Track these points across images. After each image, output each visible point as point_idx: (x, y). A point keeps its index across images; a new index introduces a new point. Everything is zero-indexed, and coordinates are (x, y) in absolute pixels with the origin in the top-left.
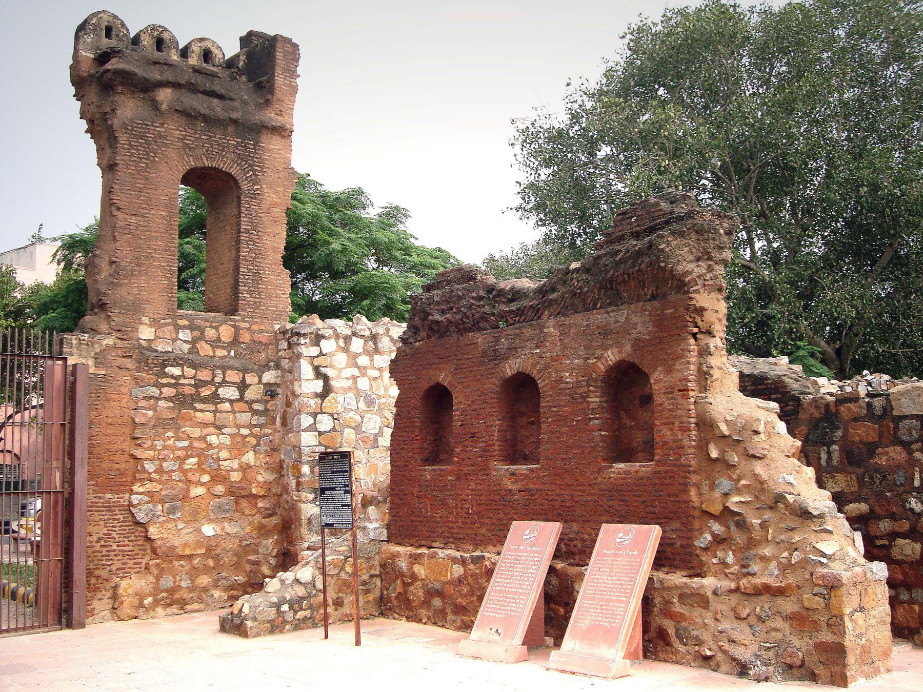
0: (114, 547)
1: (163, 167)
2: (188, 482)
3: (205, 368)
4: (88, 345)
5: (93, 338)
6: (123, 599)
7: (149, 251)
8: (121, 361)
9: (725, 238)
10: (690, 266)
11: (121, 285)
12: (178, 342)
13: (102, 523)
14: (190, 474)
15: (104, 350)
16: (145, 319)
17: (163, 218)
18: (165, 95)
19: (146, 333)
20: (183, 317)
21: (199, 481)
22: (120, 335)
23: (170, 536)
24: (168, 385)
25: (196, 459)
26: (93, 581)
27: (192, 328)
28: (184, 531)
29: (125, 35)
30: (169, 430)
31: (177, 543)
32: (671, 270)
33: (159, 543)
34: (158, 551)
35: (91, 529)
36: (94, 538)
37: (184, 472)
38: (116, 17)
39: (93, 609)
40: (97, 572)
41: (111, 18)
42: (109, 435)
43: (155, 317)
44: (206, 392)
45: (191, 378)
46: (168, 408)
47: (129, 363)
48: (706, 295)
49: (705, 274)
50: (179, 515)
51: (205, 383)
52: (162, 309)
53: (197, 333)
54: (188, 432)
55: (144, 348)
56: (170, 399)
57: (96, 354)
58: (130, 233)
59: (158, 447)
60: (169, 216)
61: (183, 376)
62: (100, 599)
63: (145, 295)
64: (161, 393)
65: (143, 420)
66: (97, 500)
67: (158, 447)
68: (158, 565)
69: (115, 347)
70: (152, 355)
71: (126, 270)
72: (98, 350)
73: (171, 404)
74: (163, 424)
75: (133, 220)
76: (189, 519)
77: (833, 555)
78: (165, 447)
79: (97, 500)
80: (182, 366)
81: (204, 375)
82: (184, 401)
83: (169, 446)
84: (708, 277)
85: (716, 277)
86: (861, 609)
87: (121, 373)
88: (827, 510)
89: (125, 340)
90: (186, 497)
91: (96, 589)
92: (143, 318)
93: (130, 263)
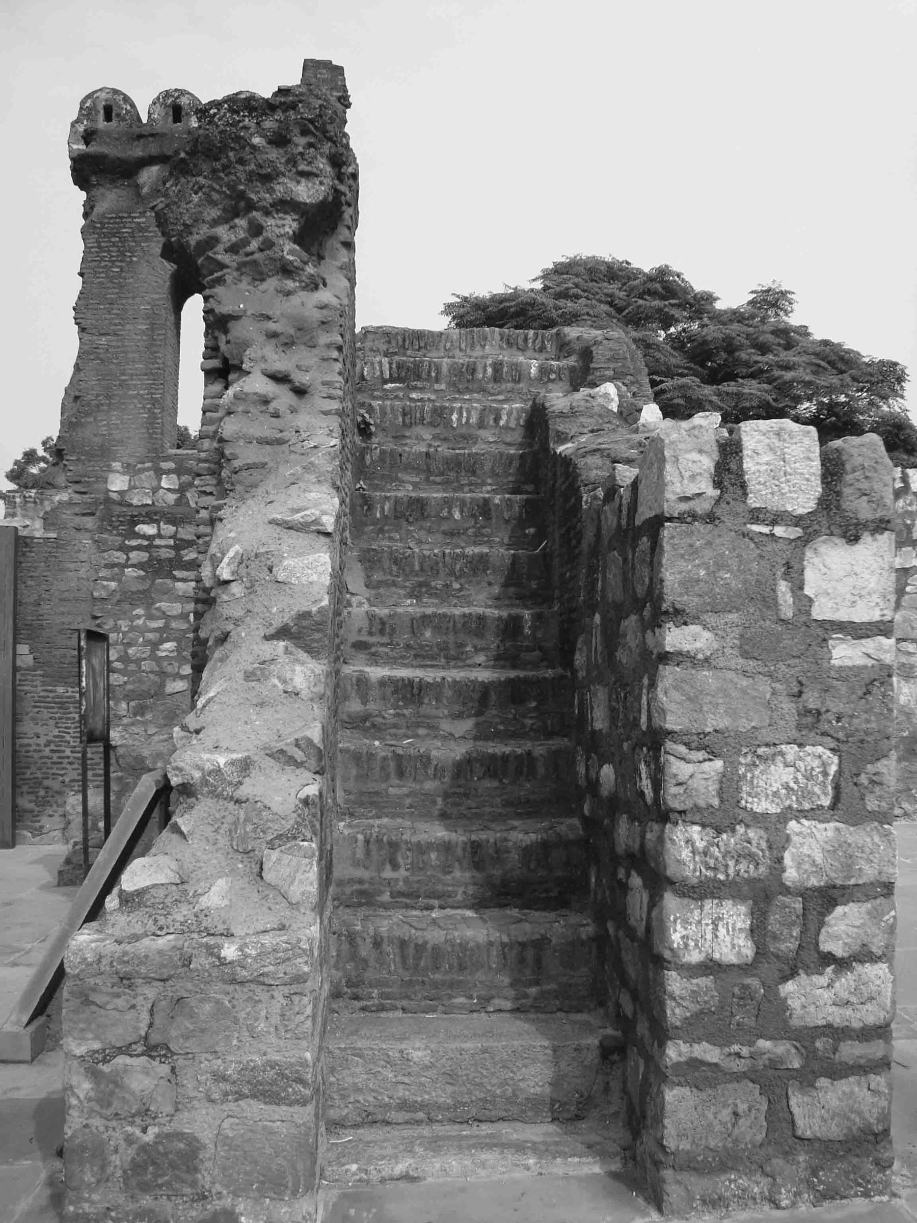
0: (68, 752)
1: (144, 270)
2: (163, 674)
3: (190, 523)
4: (35, 502)
5: (42, 494)
6: (71, 818)
7: (123, 378)
8: (78, 520)
9: (274, 154)
10: (222, 231)
11: (82, 425)
12: (161, 491)
13: (52, 722)
14: (165, 663)
15: (57, 508)
16: (116, 465)
17: (143, 333)
18: (149, 176)
19: (117, 483)
20: (167, 458)
21: (178, 673)
22: (78, 487)
23: (137, 743)
24: (139, 548)
25: (175, 644)
26: (42, 793)
27: (178, 471)
28: (156, 738)
29: (128, 112)
30: (138, 606)
31: (146, 753)
32: (181, 246)
33: (121, 751)
34: (121, 761)
35: (40, 730)
36: (42, 741)
37: (158, 660)
38: (116, 92)
39: (42, 827)
40: (46, 783)
41: (110, 96)
42: (63, 614)
43: (131, 461)
44: (190, 555)
45: (170, 537)
46: (137, 578)
47: (89, 522)
48: (244, 285)
49: (245, 242)
50: (149, 716)
51: (189, 544)
52: (141, 451)
53: (186, 478)
54: (163, 608)
55: (114, 502)
56: (140, 566)
57: (46, 513)
58: (98, 358)
59: (124, 629)
60: (152, 330)
61: (159, 536)
62: (51, 816)
63: (117, 435)
64: (128, 559)
65: (104, 594)
66: (45, 694)
67: (124, 629)
68: (120, 779)
69: (70, 503)
70: (117, 509)
71: (89, 404)
72: (48, 509)
73: (142, 573)
74: (130, 598)
75: (103, 340)
76: (162, 722)
77: (140, 893)
78: (132, 629)
79: (45, 694)
80: (157, 522)
81: (187, 533)
82: (158, 568)
83: (138, 626)
84: (254, 244)
85: (268, 245)
86: (153, 1049)
87: (79, 535)
88: (197, 775)
89: (85, 493)
90: (158, 692)
91: (44, 803)
92: (114, 464)
93: (98, 396)
